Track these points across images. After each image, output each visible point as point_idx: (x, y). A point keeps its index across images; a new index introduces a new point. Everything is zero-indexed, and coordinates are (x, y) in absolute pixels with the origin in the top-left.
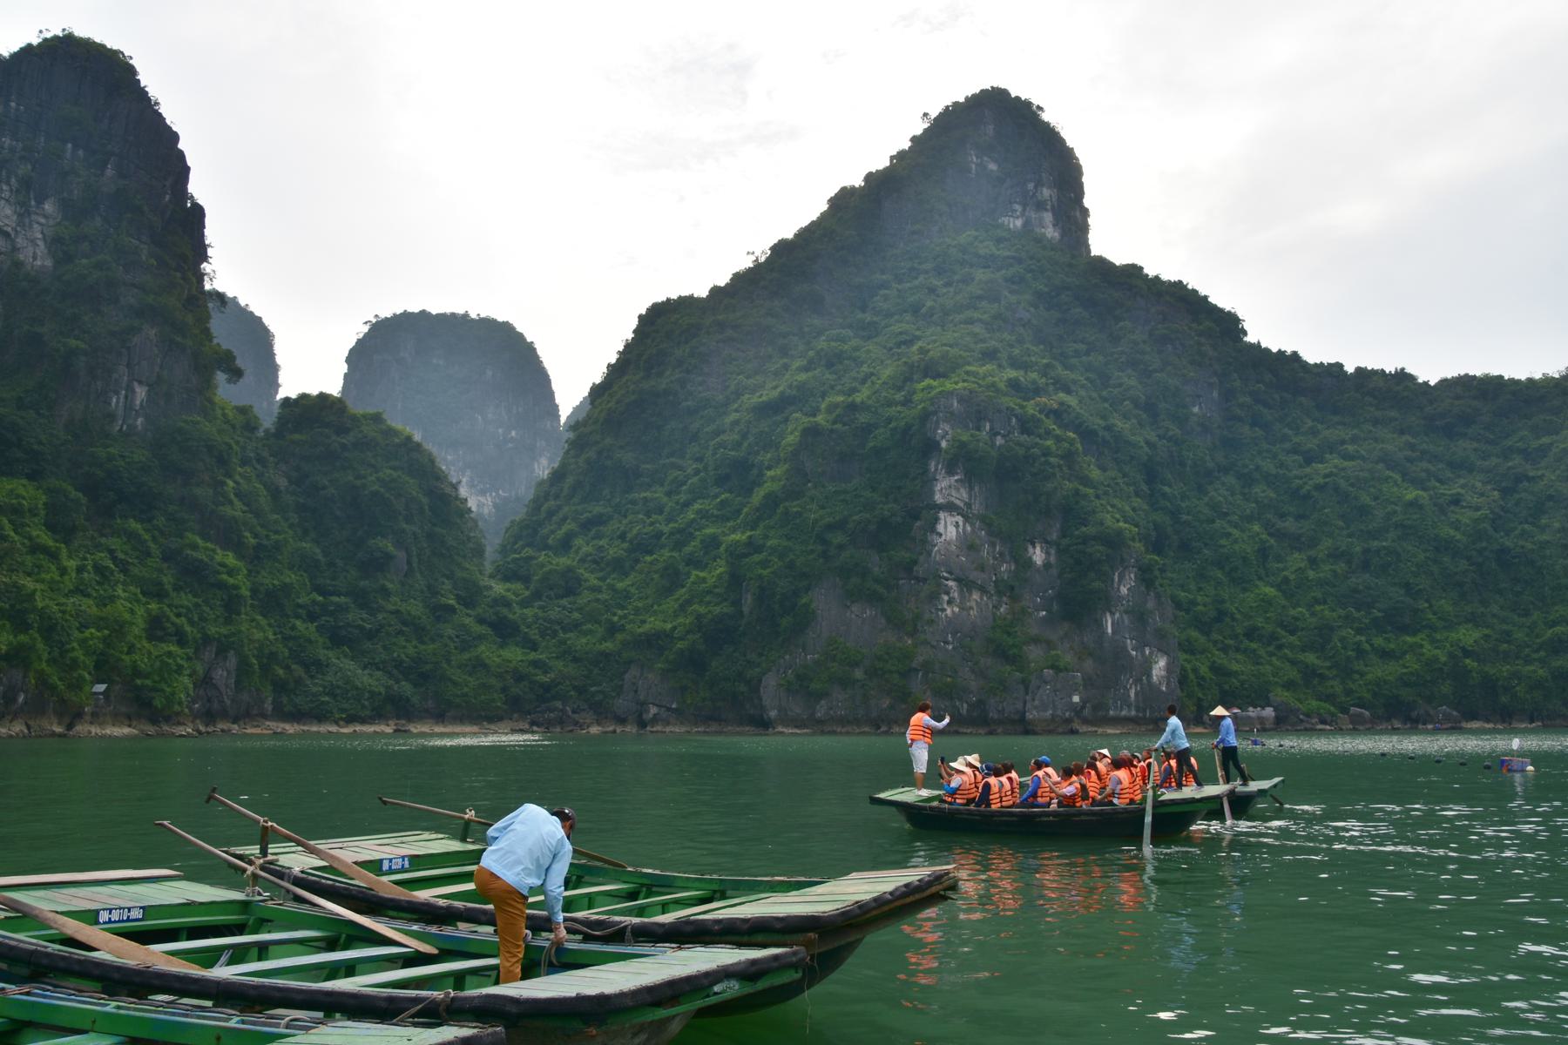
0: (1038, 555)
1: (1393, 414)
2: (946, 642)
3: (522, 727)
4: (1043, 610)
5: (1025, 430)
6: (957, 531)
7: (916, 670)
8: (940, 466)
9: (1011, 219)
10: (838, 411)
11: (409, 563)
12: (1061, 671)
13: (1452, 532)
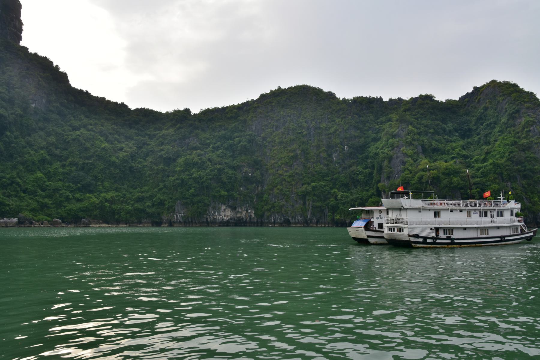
1: (114, 117)
13: (116, 159)
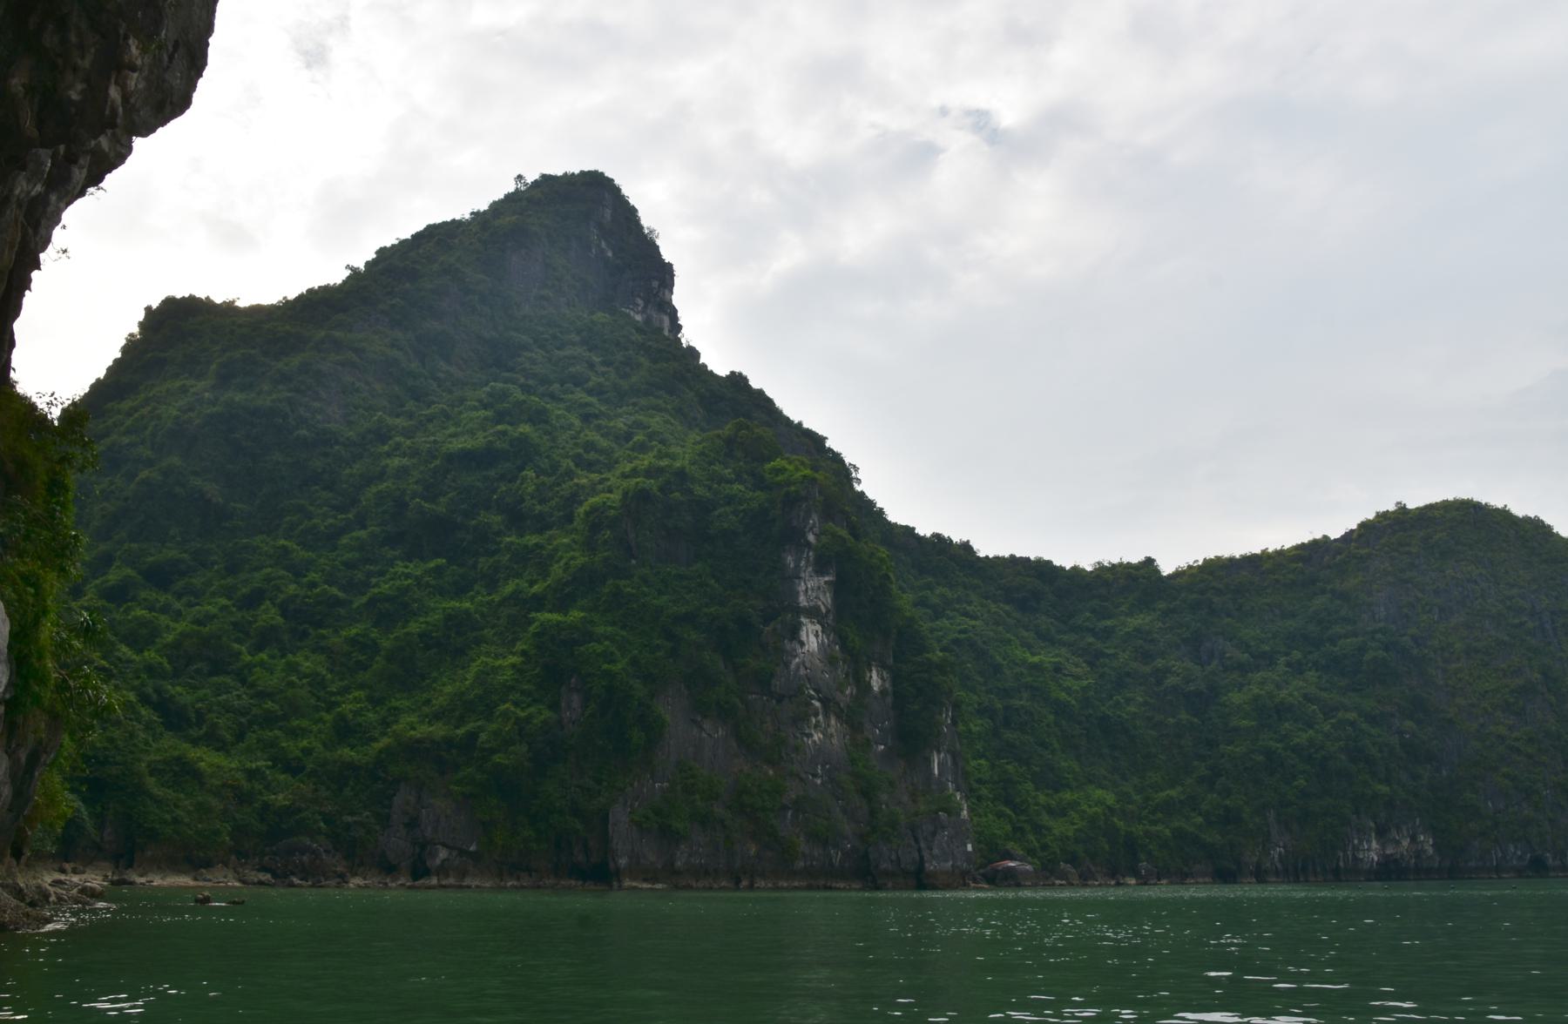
0: (875, 681)
2: (815, 775)
3: (263, 879)
4: (881, 744)
6: (818, 642)
7: (784, 808)
8: (803, 563)
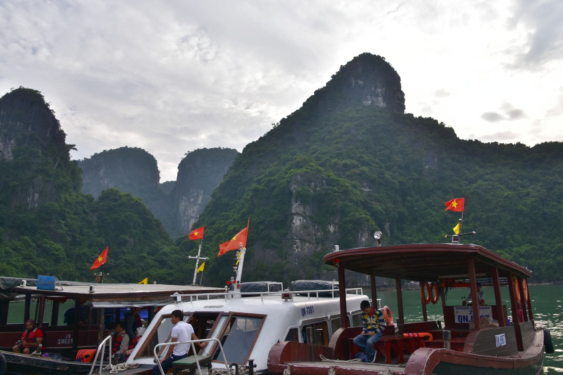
0: (332, 229)
2: (296, 262)
5: (329, 184)
6: (300, 222)
9: (367, 101)
10: (266, 182)
11: (134, 242)
12: (330, 270)
13: (523, 207)
